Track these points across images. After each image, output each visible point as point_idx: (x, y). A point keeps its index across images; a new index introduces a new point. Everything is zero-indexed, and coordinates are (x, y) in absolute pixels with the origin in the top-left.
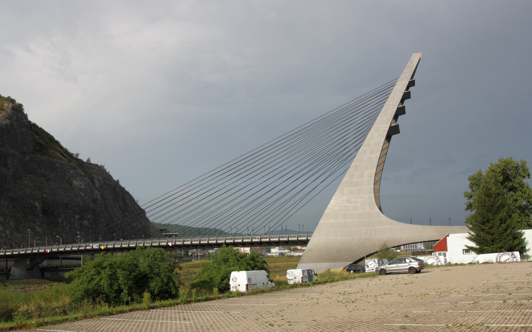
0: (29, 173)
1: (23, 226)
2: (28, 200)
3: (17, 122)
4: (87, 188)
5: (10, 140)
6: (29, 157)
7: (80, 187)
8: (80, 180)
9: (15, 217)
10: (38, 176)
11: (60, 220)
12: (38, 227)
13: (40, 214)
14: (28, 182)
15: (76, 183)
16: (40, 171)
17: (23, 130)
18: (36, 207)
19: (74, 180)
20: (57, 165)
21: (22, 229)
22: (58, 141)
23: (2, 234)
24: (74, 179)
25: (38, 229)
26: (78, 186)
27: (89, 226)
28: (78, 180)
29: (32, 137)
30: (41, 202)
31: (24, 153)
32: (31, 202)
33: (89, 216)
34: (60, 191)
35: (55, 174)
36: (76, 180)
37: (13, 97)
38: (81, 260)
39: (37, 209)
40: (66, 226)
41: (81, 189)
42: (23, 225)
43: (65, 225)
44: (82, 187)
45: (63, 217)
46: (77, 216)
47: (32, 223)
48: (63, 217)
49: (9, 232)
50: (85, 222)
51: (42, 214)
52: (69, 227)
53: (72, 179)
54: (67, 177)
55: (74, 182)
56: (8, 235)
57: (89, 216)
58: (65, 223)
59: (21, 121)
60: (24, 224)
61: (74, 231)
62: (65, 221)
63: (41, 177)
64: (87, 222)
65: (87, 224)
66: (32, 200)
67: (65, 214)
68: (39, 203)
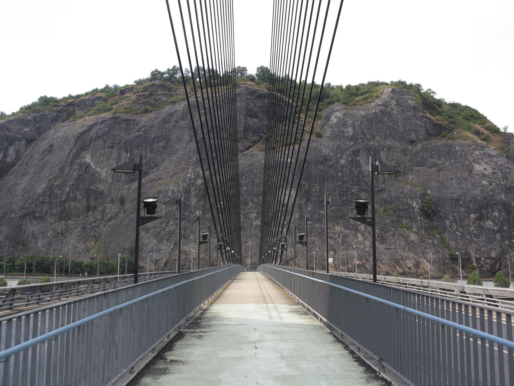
0: (418, 166)
1: (391, 234)
2: (404, 200)
3: (399, 107)
4: (495, 173)
5: (381, 130)
6: (421, 145)
7: (484, 172)
8: (487, 163)
9: (380, 224)
10: (429, 167)
11: (448, 223)
12: (414, 234)
13: (418, 217)
14: (413, 176)
15: (478, 167)
16: (432, 160)
17: (409, 113)
18: (413, 208)
19: (476, 165)
20: (457, 148)
21: (389, 238)
22: (33, 103)
23: (360, 246)
24: (477, 163)
25: (413, 237)
26: (481, 171)
27: (496, 228)
28: (483, 163)
29: (425, 119)
30: (420, 201)
31: (412, 142)
32: (409, 202)
33: (496, 214)
34: (453, 182)
35: (453, 161)
36: (479, 164)
37: (403, 80)
38: (135, 283)
39: (414, 210)
40: (457, 230)
41: (486, 175)
42: (391, 233)
43: (454, 229)
44: (486, 173)
45: (451, 218)
46: (472, 216)
47: (406, 230)
48: (451, 218)
49: (369, 243)
50: (489, 223)
51: (420, 217)
52: (460, 232)
53: (473, 164)
54: (467, 162)
55: (477, 166)
56: (367, 247)
57: (496, 214)
58: (455, 227)
59: (404, 104)
60: (393, 232)
61: (469, 237)
62: (454, 224)
63: (433, 167)
64: (491, 223)
65: (491, 225)
66: (409, 200)
67: (455, 214)
68: (417, 203)
